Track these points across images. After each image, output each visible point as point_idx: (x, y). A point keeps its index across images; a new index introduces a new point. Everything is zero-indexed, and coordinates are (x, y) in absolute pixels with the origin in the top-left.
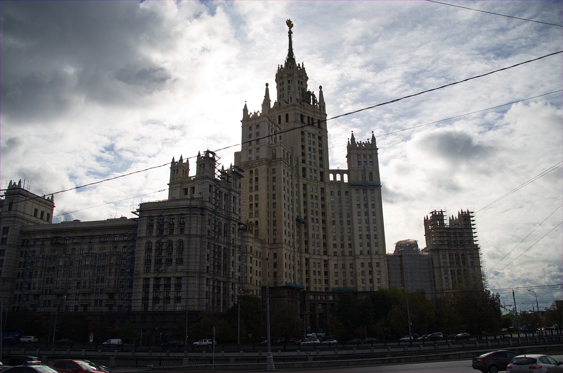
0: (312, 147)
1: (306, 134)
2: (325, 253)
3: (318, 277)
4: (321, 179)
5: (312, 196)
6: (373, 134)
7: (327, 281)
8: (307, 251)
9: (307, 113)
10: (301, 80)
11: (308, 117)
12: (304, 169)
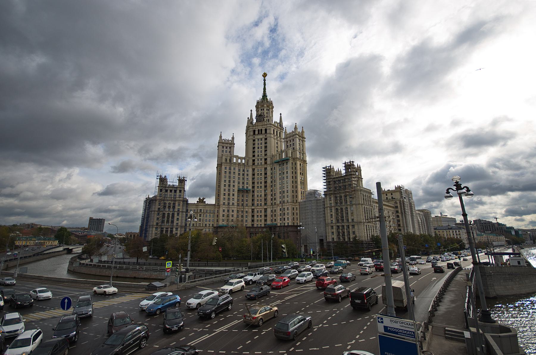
1: (256, 140)
3: (259, 218)
4: (265, 163)
5: (258, 174)
6: (296, 125)
7: (266, 220)
8: (253, 205)
9: (257, 128)
11: (259, 130)
12: (254, 160)
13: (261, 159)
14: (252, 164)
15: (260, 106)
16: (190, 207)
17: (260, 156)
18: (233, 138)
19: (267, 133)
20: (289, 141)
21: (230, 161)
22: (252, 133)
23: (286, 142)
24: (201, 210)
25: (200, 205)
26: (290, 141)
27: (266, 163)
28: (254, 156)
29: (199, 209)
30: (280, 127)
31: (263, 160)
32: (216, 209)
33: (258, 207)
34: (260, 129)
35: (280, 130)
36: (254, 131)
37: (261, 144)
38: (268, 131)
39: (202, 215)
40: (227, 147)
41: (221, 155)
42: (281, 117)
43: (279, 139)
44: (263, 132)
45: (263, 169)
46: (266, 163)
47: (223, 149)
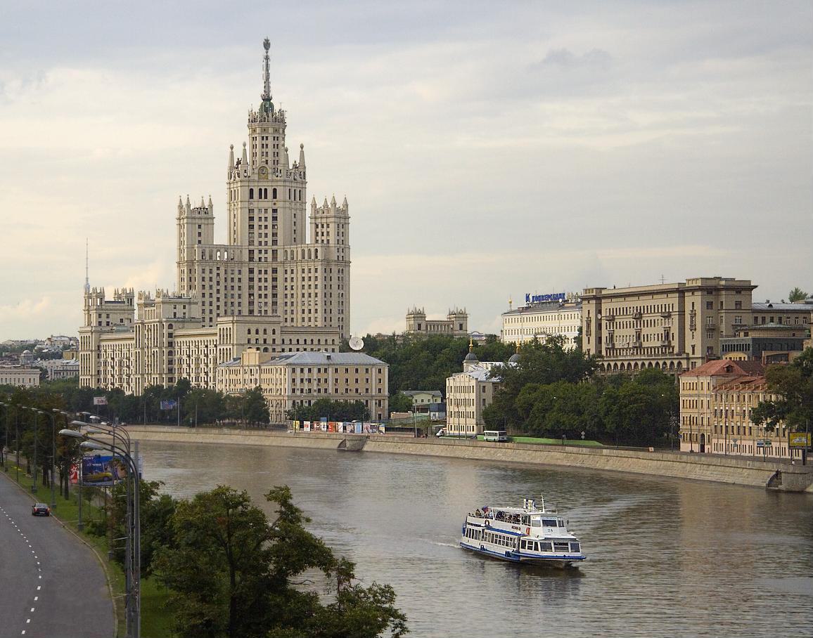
0: (263, 223)
10: (265, 135)
11: (260, 190)
14: (247, 260)
18: (211, 206)
21: (211, 257)
23: (314, 226)
26: (323, 227)
27: (275, 258)
31: (270, 252)
36: (251, 191)
42: (302, 153)
45: (270, 271)
46: (275, 258)
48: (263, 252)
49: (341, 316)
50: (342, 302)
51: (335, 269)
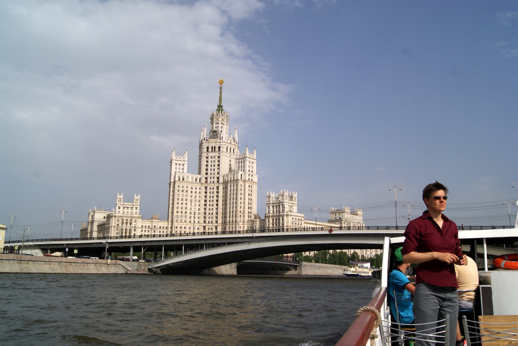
1: (210, 158)
2: (217, 222)
8: (205, 222)
9: (210, 145)
10: (217, 122)
11: (212, 147)
12: (206, 178)
13: (214, 177)
14: (204, 182)
15: (214, 120)
16: (145, 223)
17: (212, 174)
19: (220, 151)
20: (240, 163)
22: (205, 150)
24: (155, 226)
25: (154, 222)
26: (241, 162)
27: (218, 182)
28: (207, 174)
29: (154, 225)
30: (235, 143)
31: (216, 178)
32: (170, 226)
33: (209, 224)
34: (213, 147)
35: (234, 147)
36: (208, 148)
37: (214, 162)
38: (221, 149)
39: (156, 231)
40: (180, 165)
41: (174, 173)
43: (232, 156)
44: (217, 149)
45: (215, 188)
46: (218, 182)
47: (176, 166)
48: (212, 178)
49: (250, 210)
50: (251, 203)
51: (247, 185)
